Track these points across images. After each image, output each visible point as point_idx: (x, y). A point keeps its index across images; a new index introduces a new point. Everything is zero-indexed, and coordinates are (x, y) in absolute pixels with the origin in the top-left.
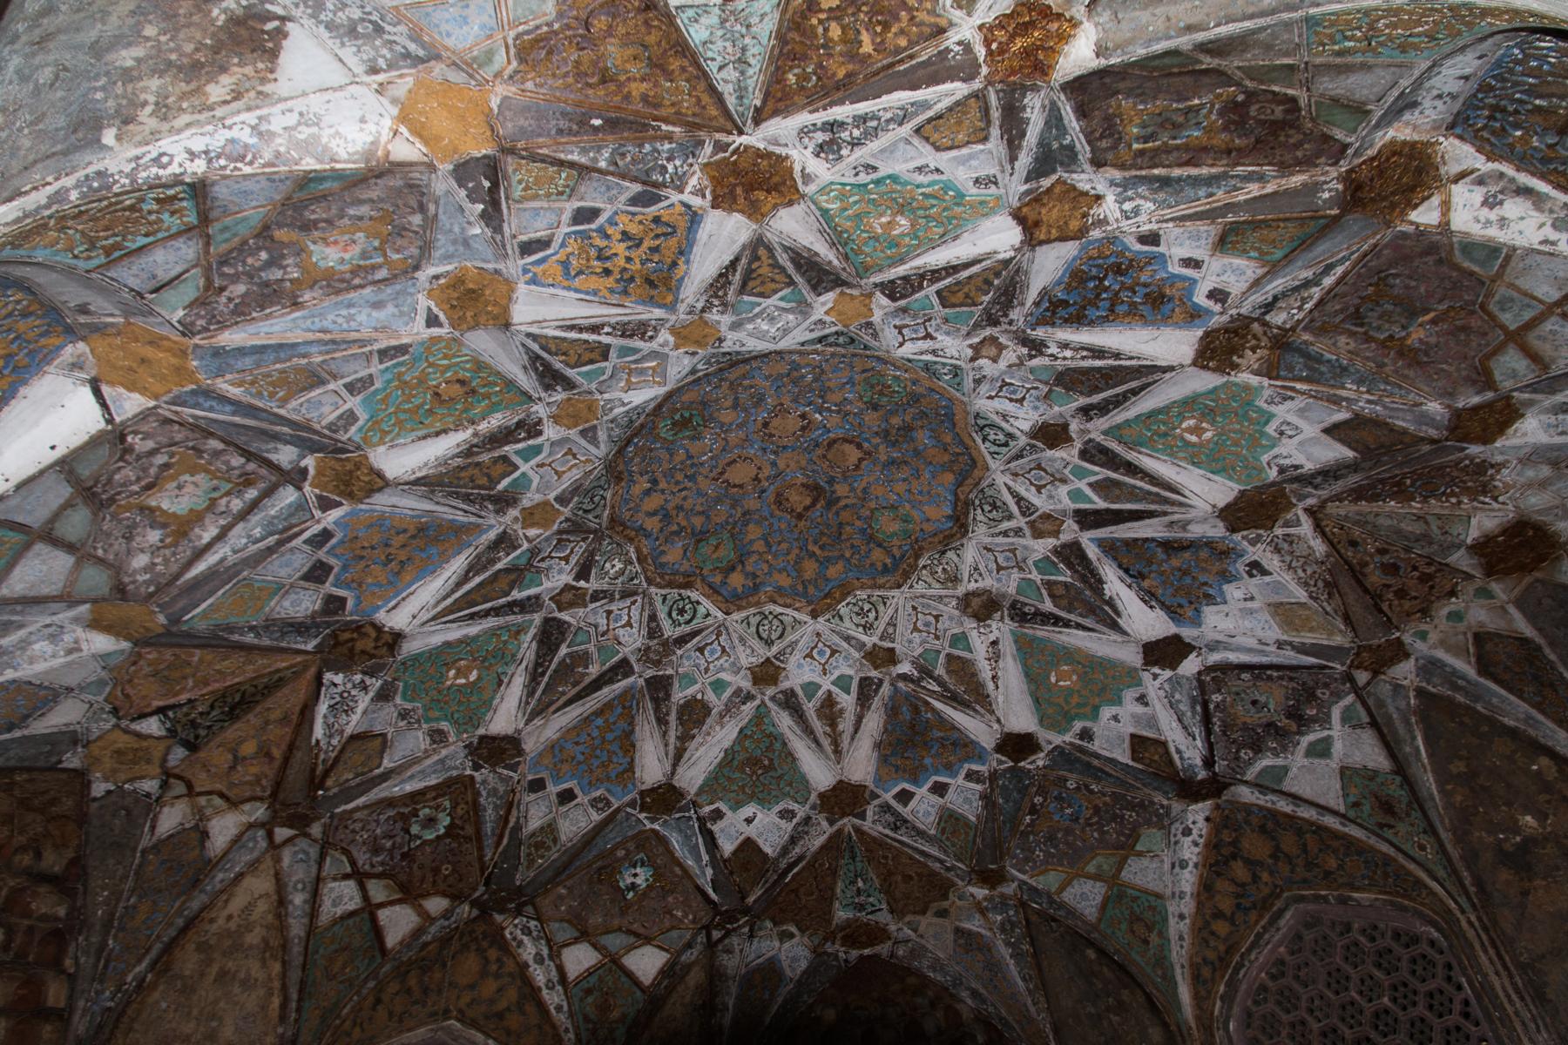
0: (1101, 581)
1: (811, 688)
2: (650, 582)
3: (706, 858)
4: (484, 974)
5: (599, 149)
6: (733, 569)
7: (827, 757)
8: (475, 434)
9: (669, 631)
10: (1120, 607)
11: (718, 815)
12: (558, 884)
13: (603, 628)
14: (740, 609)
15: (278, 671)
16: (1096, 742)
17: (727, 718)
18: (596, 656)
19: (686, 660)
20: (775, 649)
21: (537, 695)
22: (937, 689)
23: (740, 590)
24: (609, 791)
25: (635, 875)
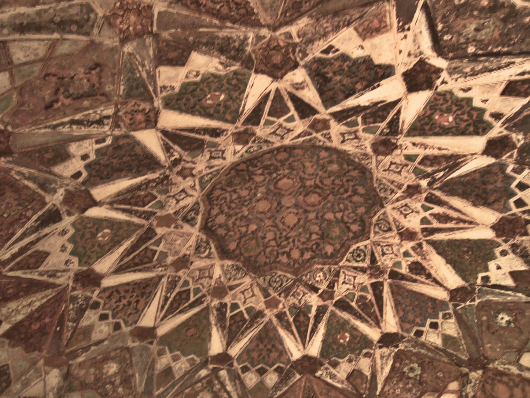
0: (359, 106)
1: (424, 221)
2: (336, 263)
3: (510, 293)
4: (511, 389)
5: (68, 327)
6: (348, 228)
7: (473, 228)
8: (216, 325)
9: (364, 265)
10: (379, 100)
11: (486, 279)
12: (483, 345)
13: (351, 287)
14: (369, 232)
15: (305, 386)
16: (505, 112)
17: (428, 257)
18: (363, 294)
19: (386, 262)
20: (394, 228)
21: (369, 319)
22: (442, 173)
23: (360, 228)
24: (441, 311)
25: (502, 318)
